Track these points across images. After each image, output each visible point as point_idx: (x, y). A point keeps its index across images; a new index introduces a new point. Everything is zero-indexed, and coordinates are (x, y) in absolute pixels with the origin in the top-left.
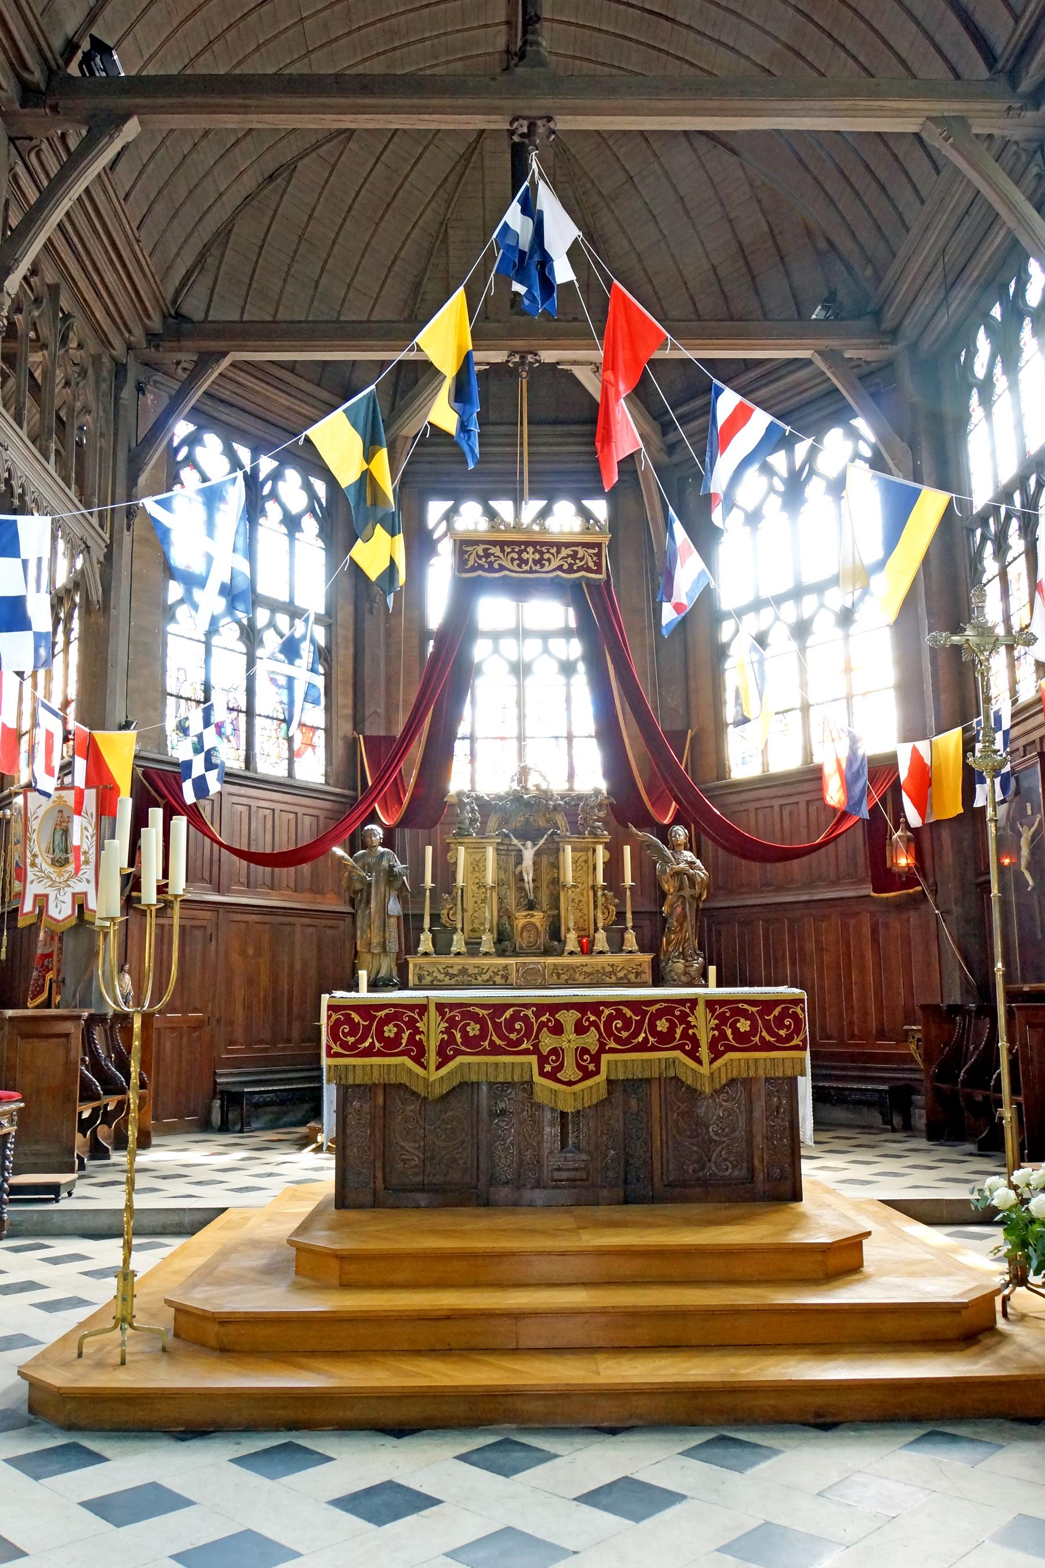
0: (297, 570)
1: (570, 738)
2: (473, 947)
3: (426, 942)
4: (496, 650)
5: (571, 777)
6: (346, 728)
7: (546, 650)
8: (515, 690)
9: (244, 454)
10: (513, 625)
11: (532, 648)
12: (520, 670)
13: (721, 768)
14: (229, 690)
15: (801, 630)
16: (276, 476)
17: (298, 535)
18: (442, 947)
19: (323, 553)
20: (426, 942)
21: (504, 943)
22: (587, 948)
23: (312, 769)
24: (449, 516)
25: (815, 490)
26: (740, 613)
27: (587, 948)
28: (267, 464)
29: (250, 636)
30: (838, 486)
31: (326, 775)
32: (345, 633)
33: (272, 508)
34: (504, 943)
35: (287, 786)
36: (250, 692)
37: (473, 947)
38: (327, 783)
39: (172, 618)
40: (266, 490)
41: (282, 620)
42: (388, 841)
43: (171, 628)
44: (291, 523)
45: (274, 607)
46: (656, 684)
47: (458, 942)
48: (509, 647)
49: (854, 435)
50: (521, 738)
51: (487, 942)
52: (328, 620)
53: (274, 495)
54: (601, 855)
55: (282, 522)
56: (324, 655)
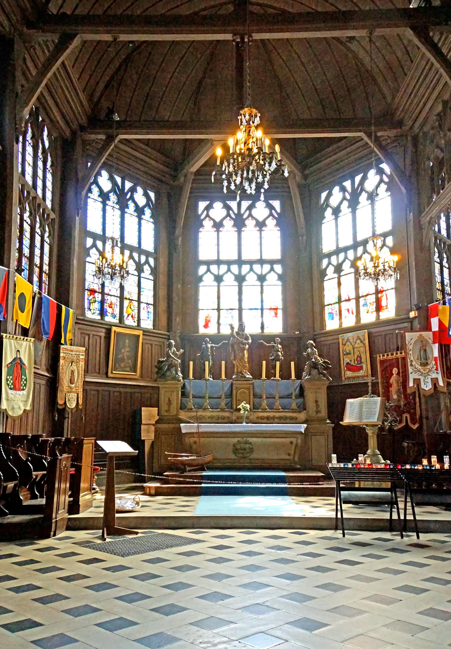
1: (262, 309)
4: (229, 270)
5: (262, 327)
7: (251, 270)
8: (237, 288)
9: (119, 180)
10: (236, 257)
11: (245, 268)
16: (133, 190)
17: (143, 216)
19: (153, 226)
24: (208, 208)
28: (128, 185)
31: (154, 326)
32: (163, 260)
38: (154, 329)
39: (89, 255)
40: (128, 197)
41: (136, 255)
43: (88, 259)
44: (140, 211)
45: (132, 249)
48: (235, 268)
50: (240, 310)
53: (132, 198)
55: (135, 211)
56: (154, 271)
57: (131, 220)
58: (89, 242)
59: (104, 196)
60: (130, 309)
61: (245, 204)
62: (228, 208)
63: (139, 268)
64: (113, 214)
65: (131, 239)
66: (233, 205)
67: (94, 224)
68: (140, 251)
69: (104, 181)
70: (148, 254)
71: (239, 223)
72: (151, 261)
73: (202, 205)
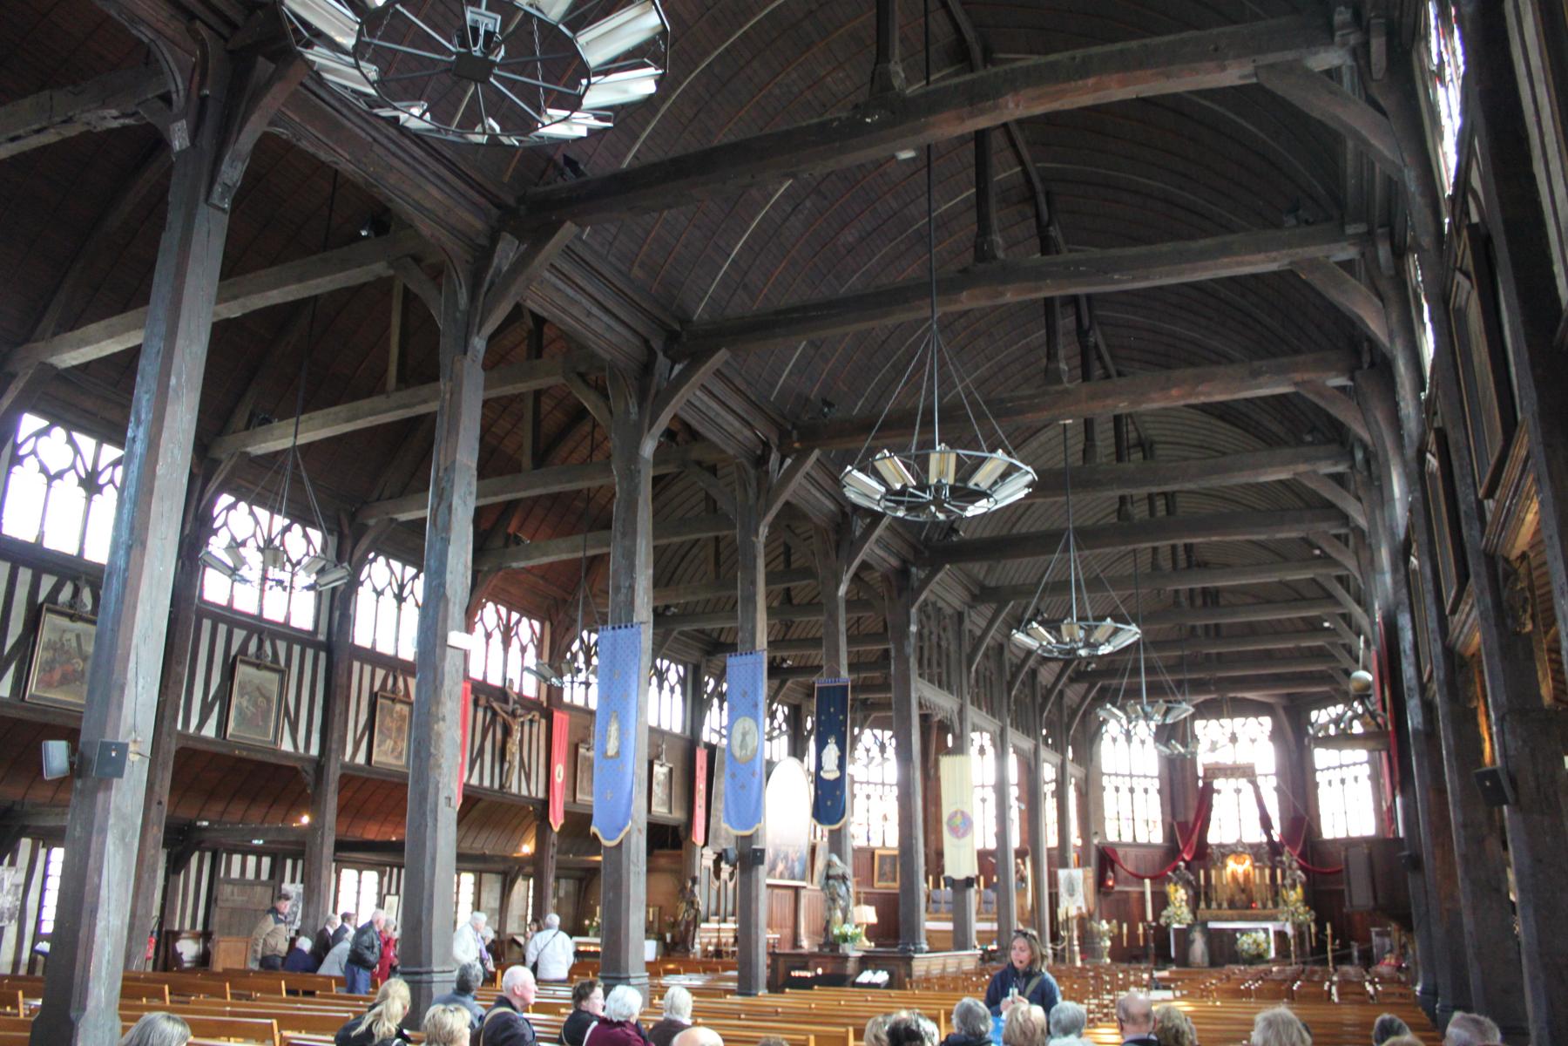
2: (1220, 906)
3: (1202, 905)
6: (1169, 819)
13: (1320, 834)
14: (1126, 812)
18: (1208, 906)
20: (1202, 905)
21: (1232, 904)
22: (1264, 907)
23: (1157, 837)
27: (1264, 907)
29: (1132, 790)
33: (1135, 740)
34: (1232, 904)
35: (1149, 846)
37: (1220, 906)
42: (1188, 866)
44: (1143, 742)
47: (1214, 905)
51: (1225, 905)
52: (1160, 777)
54: (1267, 872)
56: (1160, 791)
58: (1105, 781)
61: (1239, 721)
72: (1156, 784)
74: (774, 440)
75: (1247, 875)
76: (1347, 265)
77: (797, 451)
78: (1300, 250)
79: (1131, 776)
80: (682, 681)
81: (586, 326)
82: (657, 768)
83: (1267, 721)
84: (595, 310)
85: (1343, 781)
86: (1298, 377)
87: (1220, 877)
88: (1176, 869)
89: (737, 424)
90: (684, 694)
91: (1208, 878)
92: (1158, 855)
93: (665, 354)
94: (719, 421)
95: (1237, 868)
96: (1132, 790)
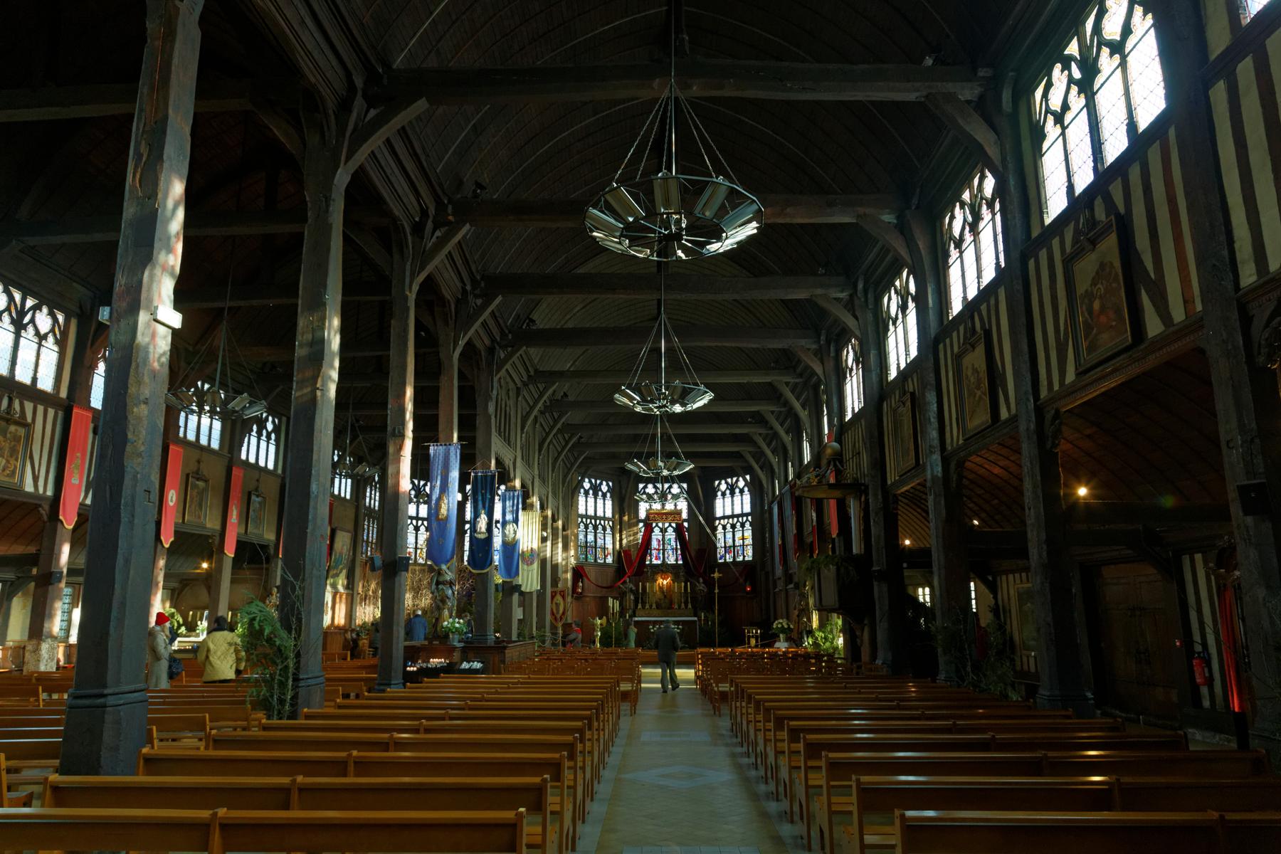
0: (606, 508)
12: (663, 531)
15: (733, 526)
18: (643, 607)
21: (658, 607)
23: (609, 560)
25: (737, 491)
26: (720, 519)
29: (595, 528)
30: (742, 491)
36: (596, 541)
44: (604, 495)
45: (600, 518)
46: (697, 540)
49: (745, 480)
52: (613, 519)
57: (600, 502)
59: (586, 493)
60: (600, 554)
61: (666, 486)
62: (655, 487)
63: (604, 529)
64: (591, 500)
65: (600, 513)
66: (659, 486)
67: (582, 510)
68: (604, 518)
69: (587, 485)
70: (609, 520)
71: (663, 497)
73: (641, 486)
74: (432, 211)
75: (669, 586)
76: (968, 102)
77: (450, 222)
78: (939, 84)
79: (595, 517)
80: (276, 429)
81: (298, 37)
82: (253, 497)
83: (685, 486)
84: (309, 21)
85: (733, 526)
86: (861, 210)
87: (652, 587)
88: (624, 582)
89: (406, 187)
90: (277, 440)
91: (644, 588)
92: (612, 570)
93: (365, 96)
94: (393, 179)
95: (664, 582)
96: (595, 528)
